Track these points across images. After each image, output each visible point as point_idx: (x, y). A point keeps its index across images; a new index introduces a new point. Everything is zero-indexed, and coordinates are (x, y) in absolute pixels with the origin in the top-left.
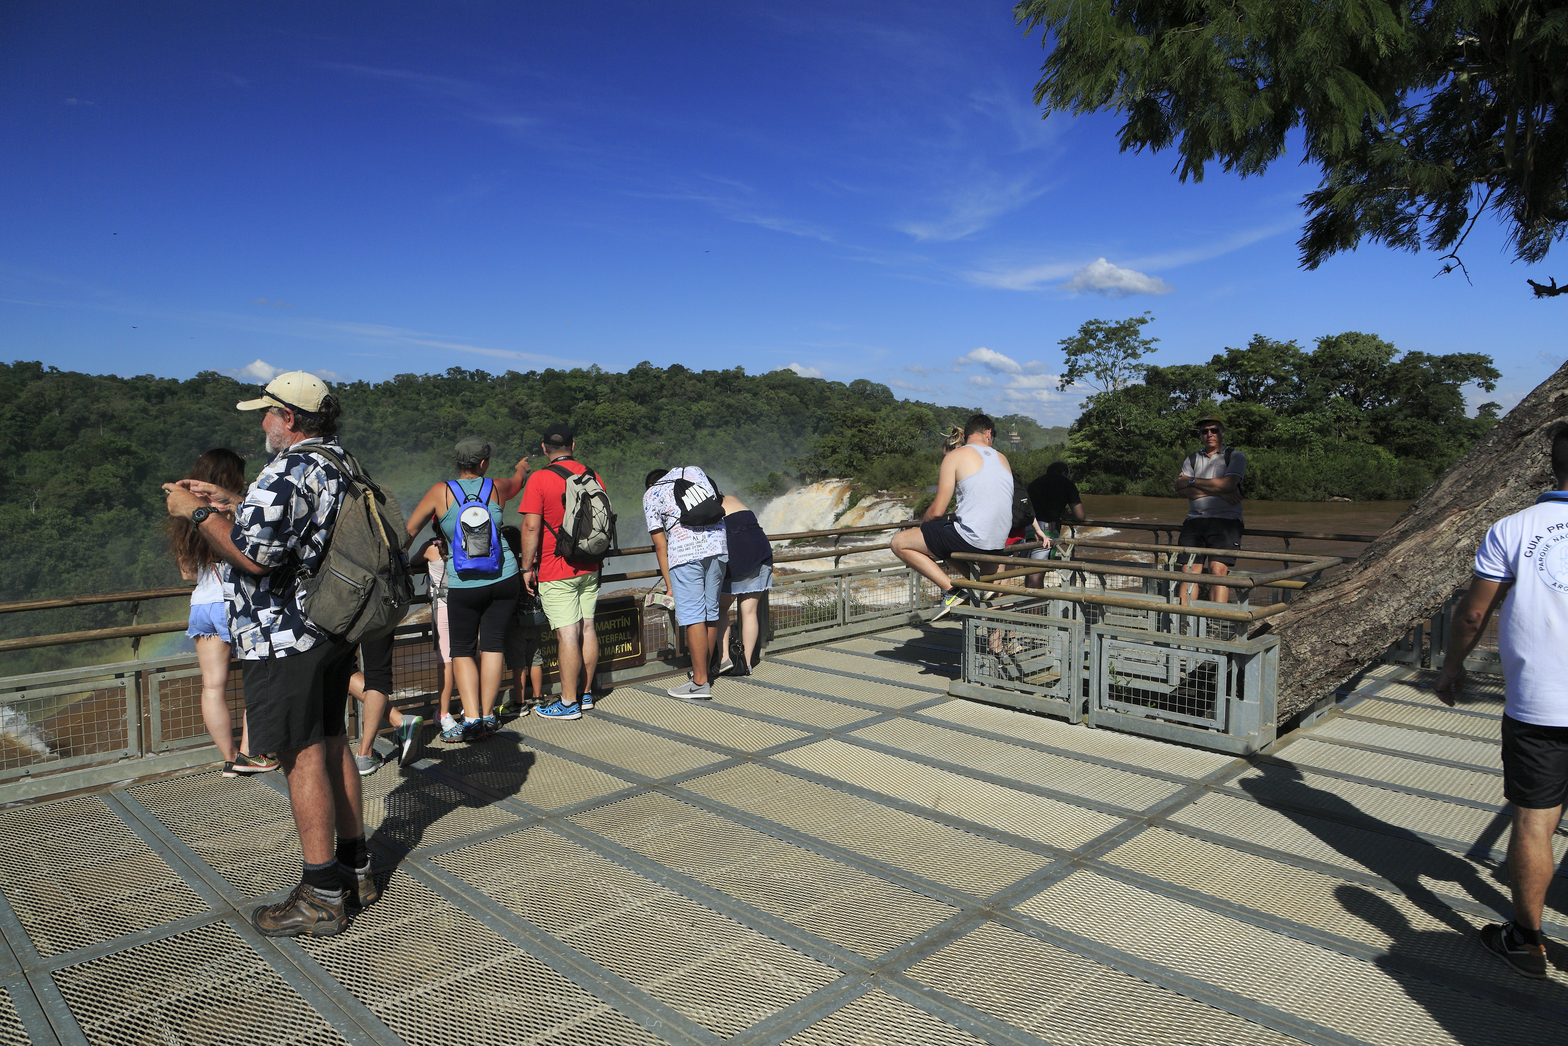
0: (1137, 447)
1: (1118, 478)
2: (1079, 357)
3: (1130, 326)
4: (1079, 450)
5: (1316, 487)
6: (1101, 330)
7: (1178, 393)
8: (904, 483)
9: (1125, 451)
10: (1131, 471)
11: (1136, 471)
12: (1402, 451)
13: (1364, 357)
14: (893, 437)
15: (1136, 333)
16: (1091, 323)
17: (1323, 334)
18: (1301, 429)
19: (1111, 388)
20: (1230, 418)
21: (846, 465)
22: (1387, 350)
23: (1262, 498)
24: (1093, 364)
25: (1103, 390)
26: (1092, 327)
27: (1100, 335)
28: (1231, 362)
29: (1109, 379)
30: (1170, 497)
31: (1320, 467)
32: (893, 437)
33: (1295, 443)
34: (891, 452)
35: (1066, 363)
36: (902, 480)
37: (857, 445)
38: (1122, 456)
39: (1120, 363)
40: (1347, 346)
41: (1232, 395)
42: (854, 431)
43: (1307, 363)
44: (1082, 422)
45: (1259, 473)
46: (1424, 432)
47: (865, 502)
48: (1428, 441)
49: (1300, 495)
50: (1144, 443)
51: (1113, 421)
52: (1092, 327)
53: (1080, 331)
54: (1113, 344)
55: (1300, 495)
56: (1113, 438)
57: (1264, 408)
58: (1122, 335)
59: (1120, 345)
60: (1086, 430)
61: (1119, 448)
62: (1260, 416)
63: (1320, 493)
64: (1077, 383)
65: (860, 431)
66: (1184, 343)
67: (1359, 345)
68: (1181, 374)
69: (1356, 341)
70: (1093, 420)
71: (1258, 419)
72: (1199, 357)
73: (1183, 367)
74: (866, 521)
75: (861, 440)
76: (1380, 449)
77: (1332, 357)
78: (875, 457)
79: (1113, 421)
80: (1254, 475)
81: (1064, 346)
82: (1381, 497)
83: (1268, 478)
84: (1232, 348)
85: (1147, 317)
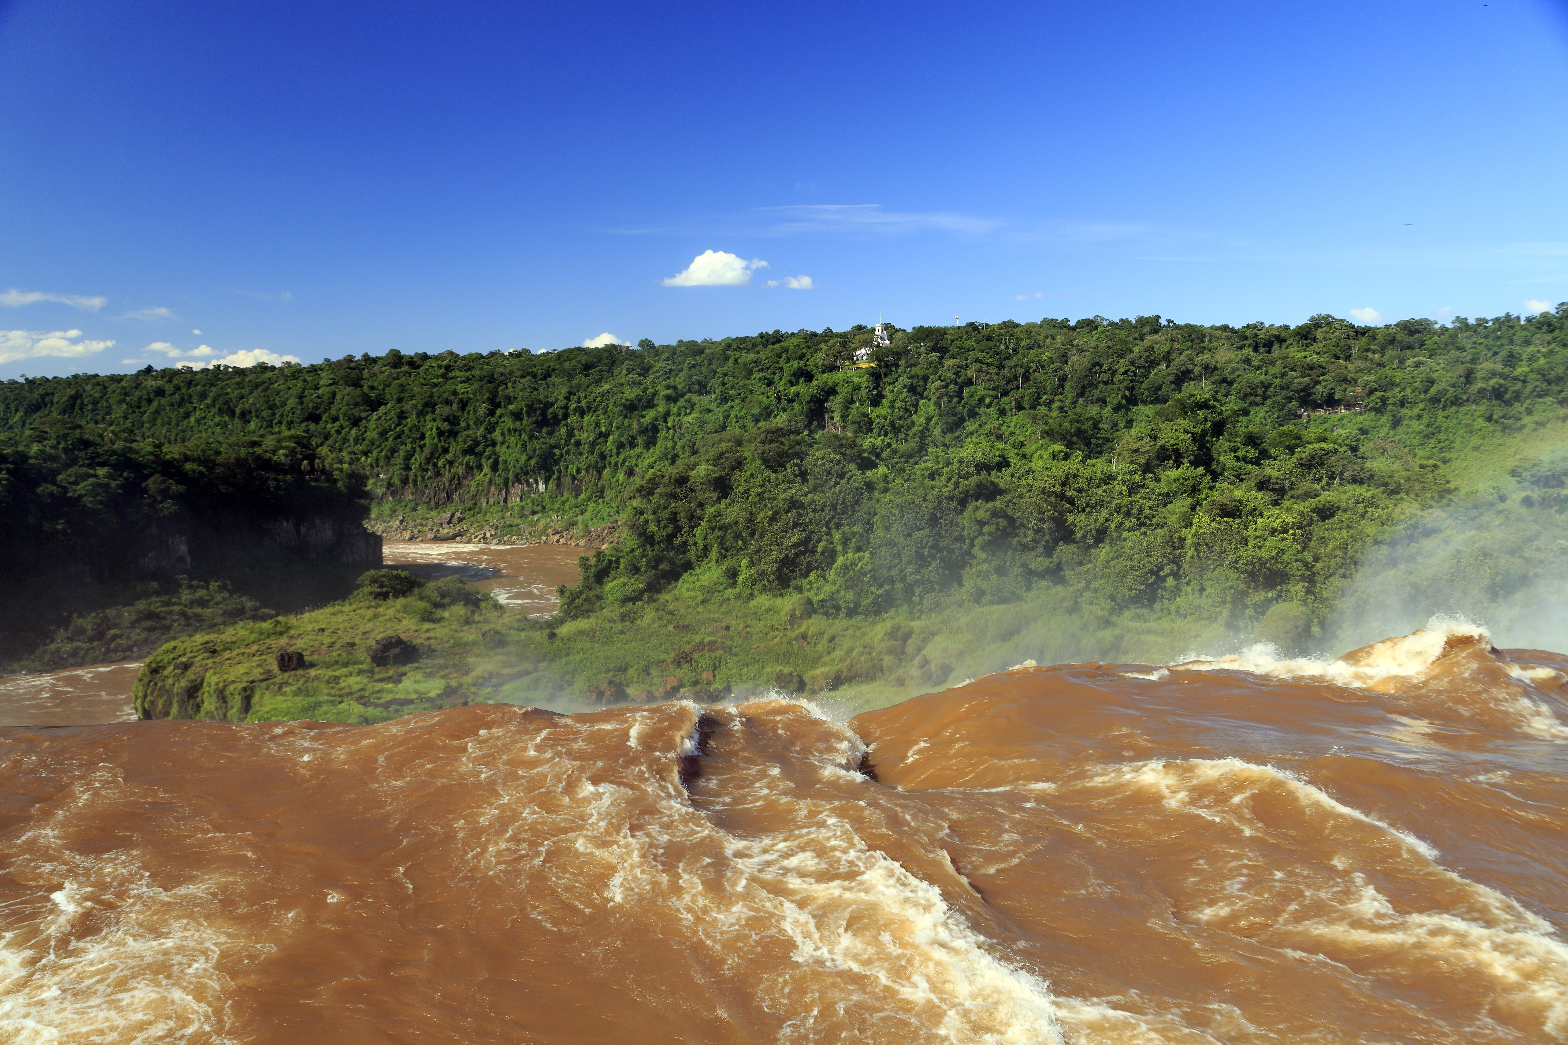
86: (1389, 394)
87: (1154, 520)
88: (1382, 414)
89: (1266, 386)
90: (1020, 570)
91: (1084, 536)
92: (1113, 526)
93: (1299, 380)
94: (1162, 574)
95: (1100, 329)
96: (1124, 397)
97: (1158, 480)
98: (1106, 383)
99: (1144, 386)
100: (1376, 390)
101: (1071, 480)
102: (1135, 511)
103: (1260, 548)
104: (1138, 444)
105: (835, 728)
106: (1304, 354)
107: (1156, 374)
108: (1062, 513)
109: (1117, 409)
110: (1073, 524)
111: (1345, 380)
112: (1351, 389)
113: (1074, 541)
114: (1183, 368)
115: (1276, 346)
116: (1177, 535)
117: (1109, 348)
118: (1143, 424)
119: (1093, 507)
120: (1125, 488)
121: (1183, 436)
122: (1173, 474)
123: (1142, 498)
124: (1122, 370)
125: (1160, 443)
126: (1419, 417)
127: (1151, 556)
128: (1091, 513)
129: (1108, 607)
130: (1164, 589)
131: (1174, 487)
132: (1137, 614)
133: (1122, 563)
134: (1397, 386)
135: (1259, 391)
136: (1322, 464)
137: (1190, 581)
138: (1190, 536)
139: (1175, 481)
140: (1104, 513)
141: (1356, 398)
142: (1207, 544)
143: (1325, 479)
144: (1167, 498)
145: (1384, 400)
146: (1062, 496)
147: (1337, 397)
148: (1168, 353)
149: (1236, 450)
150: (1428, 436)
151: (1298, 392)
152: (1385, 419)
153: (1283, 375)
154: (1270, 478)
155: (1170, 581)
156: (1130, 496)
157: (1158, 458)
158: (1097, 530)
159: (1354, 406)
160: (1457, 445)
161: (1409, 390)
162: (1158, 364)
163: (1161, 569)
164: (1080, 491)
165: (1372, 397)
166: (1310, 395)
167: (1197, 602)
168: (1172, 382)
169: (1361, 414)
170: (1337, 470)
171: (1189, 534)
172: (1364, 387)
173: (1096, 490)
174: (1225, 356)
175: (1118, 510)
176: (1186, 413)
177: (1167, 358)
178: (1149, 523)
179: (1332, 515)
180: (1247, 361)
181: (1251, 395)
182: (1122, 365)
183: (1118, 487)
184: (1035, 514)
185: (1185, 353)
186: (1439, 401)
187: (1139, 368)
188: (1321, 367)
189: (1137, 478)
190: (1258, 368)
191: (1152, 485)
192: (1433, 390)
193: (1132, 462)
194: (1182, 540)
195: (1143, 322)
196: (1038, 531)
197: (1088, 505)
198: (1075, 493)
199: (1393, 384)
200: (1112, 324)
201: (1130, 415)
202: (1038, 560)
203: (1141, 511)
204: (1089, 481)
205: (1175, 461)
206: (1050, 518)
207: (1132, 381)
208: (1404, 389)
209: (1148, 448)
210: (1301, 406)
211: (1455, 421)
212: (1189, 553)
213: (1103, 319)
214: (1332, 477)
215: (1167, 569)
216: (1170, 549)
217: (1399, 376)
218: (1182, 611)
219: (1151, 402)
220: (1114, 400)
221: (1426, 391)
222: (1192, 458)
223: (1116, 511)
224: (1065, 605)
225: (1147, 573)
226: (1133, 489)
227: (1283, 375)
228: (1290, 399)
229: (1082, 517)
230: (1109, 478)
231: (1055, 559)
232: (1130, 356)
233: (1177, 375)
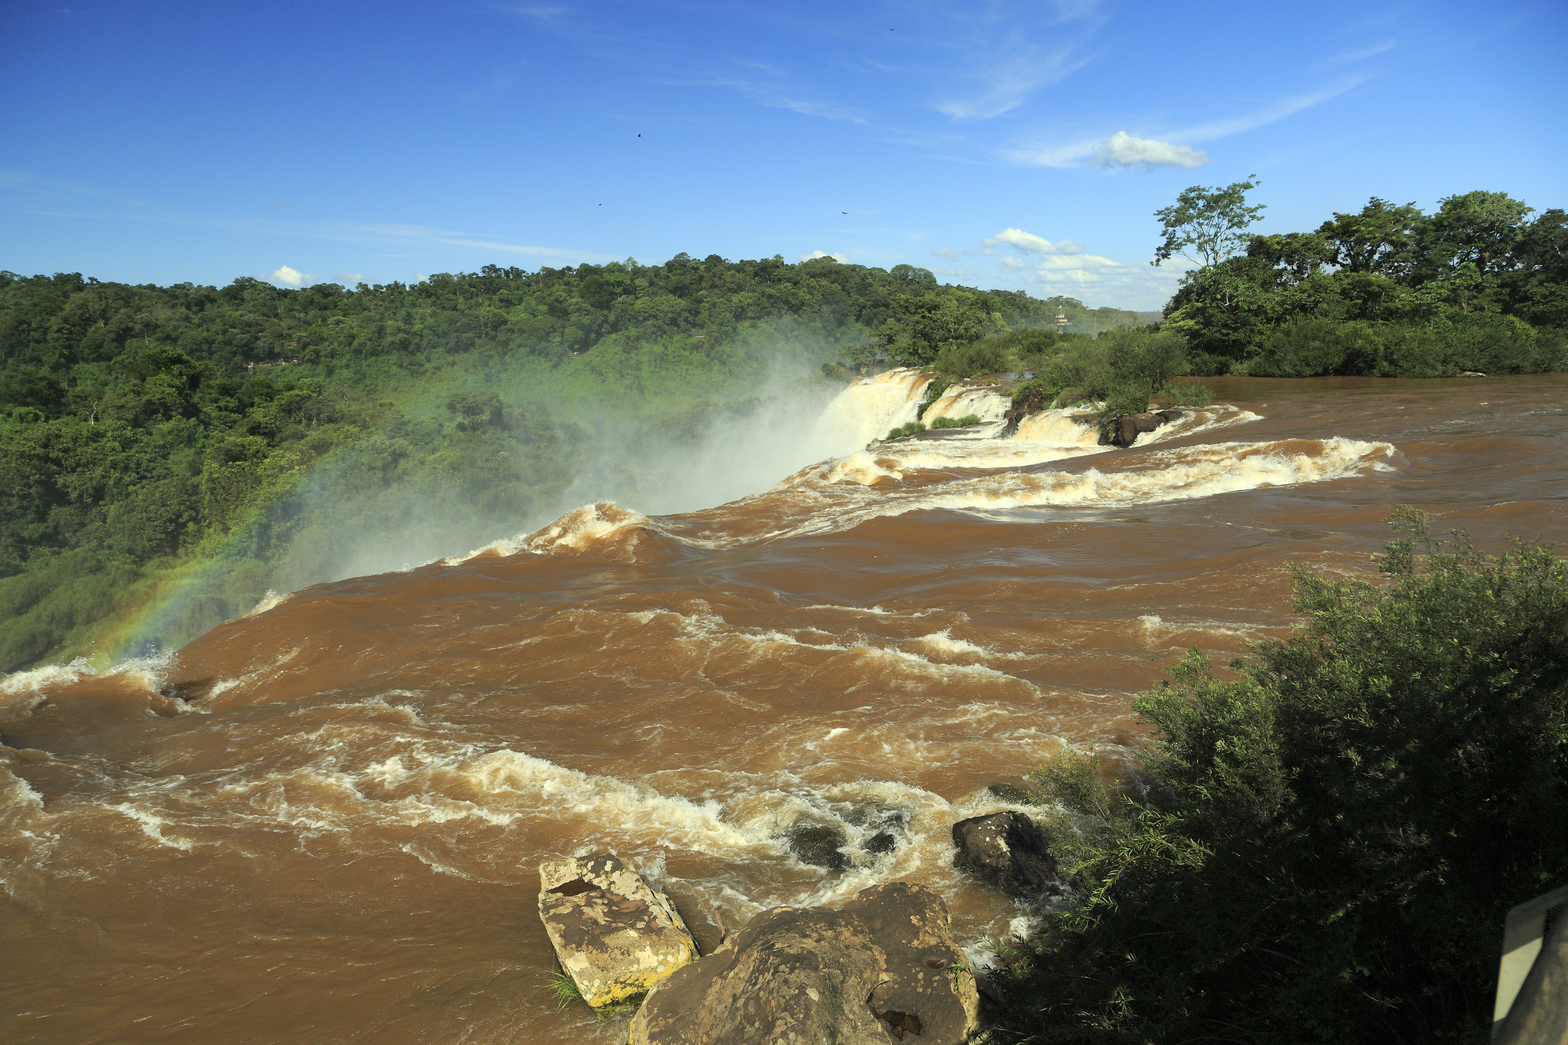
0: (1245, 324)
1: (1222, 359)
2: (1178, 229)
4: (1180, 330)
5: (1445, 362)
6: (1203, 197)
7: (1282, 265)
8: (986, 371)
10: (1238, 350)
11: (1242, 351)
12: (1536, 320)
13: (1493, 219)
15: (1241, 199)
16: (1191, 190)
17: (1448, 195)
18: (1428, 299)
19: (1211, 262)
20: (1344, 289)
21: (910, 354)
22: (1519, 209)
23: (1385, 375)
24: (1194, 235)
25: (1204, 264)
26: (1192, 195)
27: (1201, 203)
28: (1343, 229)
29: (1209, 252)
30: (1282, 376)
31: (1449, 340)
32: (959, 322)
33: (1419, 314)
34: (956, 338)
35: (1163, 235)
36: (982, 367)
37: (921, 332)
38: (1227, 335)
39: (1226, 233)
40: (1474, 208)
41: (1342, 265)
42: (917, 317)
43: (1431, 227)
44: (1179, 301)
45: (1382, 348)
47: (951, 392)
49: (1429, 371)
50: (1253, 319)
51: (1219, 297)
52: (1192, 195)
53: (1179, 200)
54: (1215, 214)
55: (1429, 371)
57: (1379, 277)
58: (1225, 202)
60: (1185, 308)
61: (1225, 326)
62: (1379, 286)
63: (1451, 368)
64: (1174, 256)
65: (924, 317)
66: (1291, 209)
67: (1487, 204)
68: (1287, 244)
69: (1483, 202)
70: (1193, 296)
71: (1377, 289)
72: (1307, 224)
73: (1289, 236)
74: (955, 413)
75: (926, 326)
76: (1511, 317)
77: (1459, 219)
78: (940, 344)
79: (1219, 297)
80: (1376, 350)
81: (1161, 217)
82: (1515, 370)
83: (1392, 354)
84: (1342, 212)
85: (1253, 182)
86: (320, 347)
87: (155, 473)
88: (317, 364)
90: (10, 540)
91: (80, 496)
92: (111, 482)
93: (241, 337)
94: (181, 520)
95: (13, 285)
96: (62, 355)
97: (151, 434)
98: (37, 342)
99: (83, 343)
100: (309, 344)
101: (53, 441)
102: (132, 465)
103: (273, 484)
104: (123, 400)
106: (239, 313)
107: (94, 332)
108: (50, 476)
109: (56, 368)
110: (64, 485)
111: (281, 336)
112: (287, 343)
113: (69, 503)
114: (123, 326)
115: (208, 306)
116: (189, 482)
117: (36, 305)
118: (89, 382)
120: (117, 444)
121: (168, 390)
122: (166, 426)
124: (55, 328)
125: (145, 398)
126: (348, 366)
127: (167, 505)
128: (83, 472)
129: (129, 561)
130: (186, 534)
131: (169, 438)
132: (162, 562)
133: (136, 516)
134: (326, 340)
135: (205, 347)
136: (300, 409)
137: (210, 523)
138: (203, 482)
139: (169, 433)
140: (98, 472)
141: (293, 351)
142: (223, 488)
145: (317, 353)
146: (46, 459)
147: (276, 350)
148: (104, 311)
150: (357, 382)
151: (241, 347)
152: (320, 368)
153: (225, 332)
155: (191, 526)
156: (124, 451)
157: (145, 412)
158: (94, 488)
159: (293, 358)
160: (380, 388)
161: (336, 344)
162: (95, 322)
163: (179, 515)
164: (66, 451)
165: (307, 351)
166: (252, 349)
167: (225, 540)
168: (113, 340)
169: (299, 365)
170: (314, 413)
171: (202, 480)
172: (298, 342)
173: (85, 449)
174: (162, 314)
176: (160, 368)
177: (104, 315)
178: (149, 475)
179: (327, 450)
180: (187, 319)
181: (197, 350)
182: (54, 323)
183: (109, 443)
184: (18, 480)
186: (360, 352)
187: (74, 326)
188: (258, 324)
189: (128, 433)
190: (199, 326)
191: (146, 439)
192: (355, 343)
193: (119, 419)
194: (196, 487)
195: (62, 279)
196: (23, 497)
197: (78, 465)
198: (61, 454)
199: (323, 339)
200: (24, 280)
201: (72, 374)
202: (31, 526)
203: (139, 464)
204: (75, 440)
205: (164, 415)
206: (36, 481)
207: (68, 339)
208: (332, 343)
209: (133, 403)
211: (376, 369)
212: (207, 498)
213: (13, 275)
214: (310, 419)
215: (186, 516)
216: (185, 497)
217: (325, 332)
218: (207, 551)
219: (94, 360)
220: (50, 358)
221: (350, 345)
222: (180, 410)
223: (111, 467)
224: (87, 565)
225: (165, 522)
226: (126, 444)
227: (225, 332)
228: (235, 354)
229: (74, 477)
230: (96, 436)
231: (51, 523)
232: (63, 314)
233: (117, 333)
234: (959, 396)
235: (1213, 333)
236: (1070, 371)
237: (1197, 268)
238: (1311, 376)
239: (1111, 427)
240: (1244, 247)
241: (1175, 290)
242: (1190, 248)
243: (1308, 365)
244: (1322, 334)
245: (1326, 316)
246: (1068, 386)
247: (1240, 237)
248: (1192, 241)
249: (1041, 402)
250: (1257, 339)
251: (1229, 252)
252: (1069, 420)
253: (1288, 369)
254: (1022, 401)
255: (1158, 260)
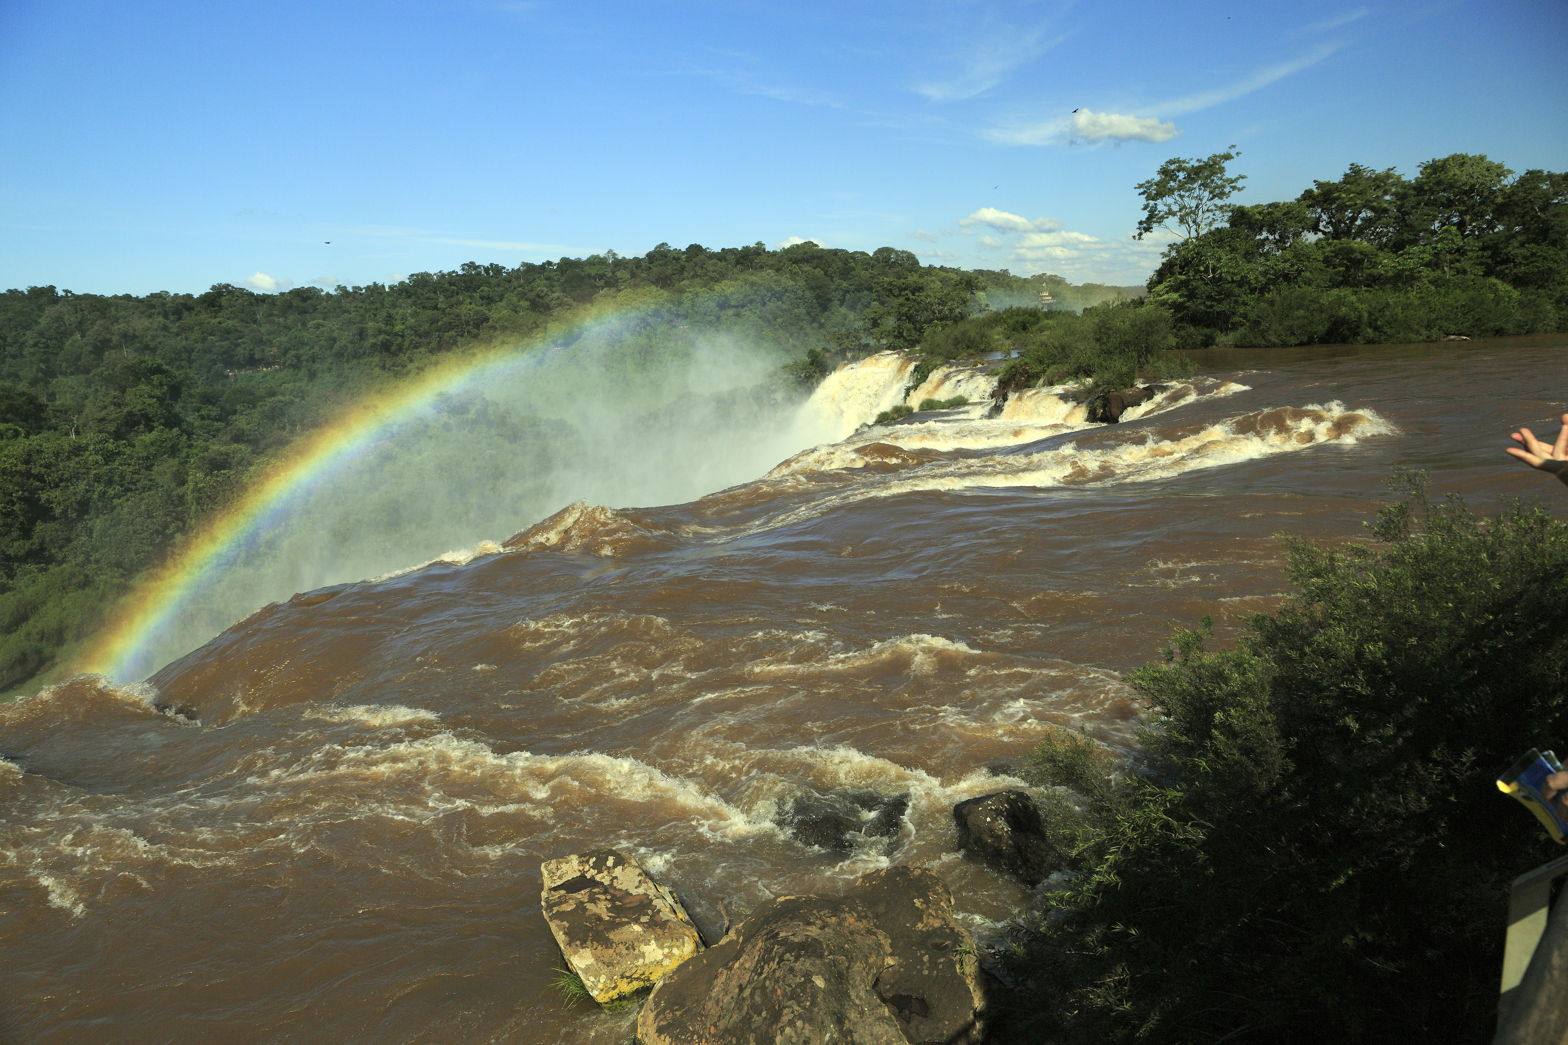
0: (1229, 295)
1: (1208, 331)
2: (1159, 202)
3: (1215, 163)
4: (1164, 303)
5: (1428, 327)
6: (1184, 169)
7: (1265, 234)
8: (971, 351)
9: (1216, 300)
10: (1223, 322)
11: (1227, 322)
12: (1518, 282)
13: (1473, 181)
14: (943, 303)
15: (1222, 170)
16: (1171, 162)
17: (1428, 159)
18: (1411, 264)
19: (1194, 234)
22: (1499, 171)
23: (1370, 342)
24: (1175, 208)
26: (1173, 167)
27: (1181, 175)
28: (1323, 197)
29: (1191, 224)
31: (1432, 305)
32: (943, 303)
33: (1402, 279)
34: (941, 319)
35: (1145, 209)
36: (968, 347)
37: (905, 314)
38: (1211, 307)
39: (1207, 204)
41: (1324, 233)
42: (901, 300)
43: (1412, 192)
44: (1162, 274)
45: (1366, 315)
46: (1545, 258)
48: (1550, 269)
49: (1413, 336)
50: (1237, 291)
51: (1202, 269)
52: (1173, 167)
53: (1159, 173)
54: (1196, 185)
55: (1413, 336)
56: (1203, 288)
57: (1360, 244)
59: (1204, 185)
60: (1169, 281)
61: (1209, 298)
62: (1361, 253)
65: (908, 299)
66: (1270, 178)
67: (1466, 167)
68: (1269, 213)
69: (1462, 164)
70: (1177, 269)
71: (1359, 256)
72: (1288, 192)
73: (1270, 206)
74: (944, 394)
76: (1493, 280)
77: (1439, 183)
78: (926, 326)
79: (1202, 269)
80: (1360, 317)
81: (1142, 190)
82: (1499, 332)
83: (1376, 320)
84: (1322, 180)
85: (1233, 152)
86: (301, 352)
87: (139, 485)
88: (299, 369)
89: (190, 351)
91: (65, 512)
92: (95, 496)
94: (168, 532)
96: (39, 370)
97: (134, 446)
98: (14, 357)
100: (289, 349)
101: (35, 456)
102: (116, 478)
104: (104, 412)
105: (1369, 434)
106: (217, 320)
107: (72, 345)
110: (48, 501)
111: (261, 342)
112: (267, 349)
113: (54, 519)
114: (101, 338)
115: (186, 314)
116: (174, 493)
117: (10, 320)
118: (68, 396)
119: (68, 480)
120: (99, 457)
121: (149, 401)
122: (148, 437)
123: (121, 464)
124: (31, 342)
125: (126, 410)
126: (330, 370)
127: (153, 517)
128: (67, 487)
131: (152, 449)
134: (307, 344)
135: (184, 356)
138: (189, 492)
139: (152, 444)
140: (82, 486)
141: (274, 357)
142: (209, 497)
143: (288, 427)
144: (148, 463)
145: (298, 357)
146: (28, 475)
147: (257, 357)
148: (81, 323)
149: (198, 410)
152: (302, 373)
154: (243, 431)
156: (106, 464)
157: (127, 424)
158: (79, 503)
159: (274, 364)
161: (317, 348)
162: (71, 335)
163: (166, 526)
164: (48, 466)
165: (288, 356)
168: (91, 352)
169: (281, 370)
172: (279, 348)
173: (67, 463)
174: (139, 324)
175: (98, 479)
176: (140, 379)
177: (81, 327)
178: (133, 487)
180: (165, 328)
181: (177, 360)
182: (30, 337)
185: (98, 323)
186: (342, 355)
187: (51, 339)
188: (237, 331)
189: (110, 446)
190: (178, 334)
191: (128, 451)
192: (337, 347)
193: (100, 432)
194: (181, 497)
195: (36, 293)
197: (61, 480)
198: (43, 470)
199: (303, 344)
202: (16, 544)
203: (122, 477)
204: (57, 455)
205: (145, 426)
206: (19, 498)
207: (44, 353)
208: (313, 347)
210: (226, 367)
215: (172, 527)
219: (72, 373)
221: (331, 348)
222: (162, 421)
223: (95, 481)
224: (74, 581)
225: (152, 534)
226: (109, 457)
227: (204, 340)
228: (214, 362)
229: (58, 492)
230: (78, 450)
231: (36, 540)
234: (947, 377)
235: (1197, 306)
236: (1056, 348)
237: (1179, 240)
238: (1296, 345)
239: (1098, 403)
240: (1226, 218)
241: (1158, 263)
242: (1172, 221)
243: (1293, 334)
244: (1306, 302)
245: (1310, 285)
246: (1054, 363)
247: (1221, 208)
248: (1174, 214)
249: (1027, 380)
250: (1242, 309)
251: (1210, 224)
252: (1056, 398)
253: (1273, 339)
254: (1009, 380)
255: (1140, 234)
